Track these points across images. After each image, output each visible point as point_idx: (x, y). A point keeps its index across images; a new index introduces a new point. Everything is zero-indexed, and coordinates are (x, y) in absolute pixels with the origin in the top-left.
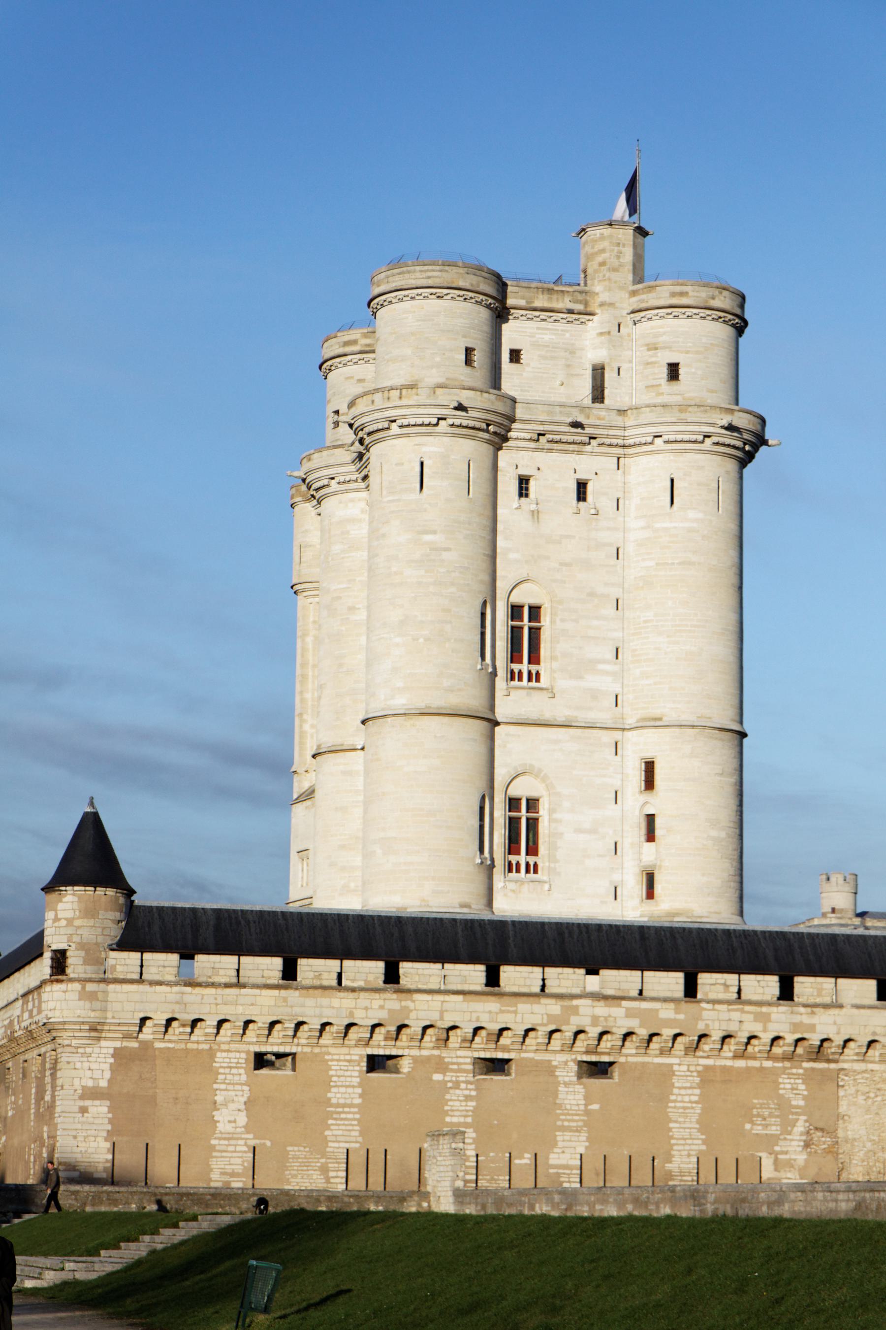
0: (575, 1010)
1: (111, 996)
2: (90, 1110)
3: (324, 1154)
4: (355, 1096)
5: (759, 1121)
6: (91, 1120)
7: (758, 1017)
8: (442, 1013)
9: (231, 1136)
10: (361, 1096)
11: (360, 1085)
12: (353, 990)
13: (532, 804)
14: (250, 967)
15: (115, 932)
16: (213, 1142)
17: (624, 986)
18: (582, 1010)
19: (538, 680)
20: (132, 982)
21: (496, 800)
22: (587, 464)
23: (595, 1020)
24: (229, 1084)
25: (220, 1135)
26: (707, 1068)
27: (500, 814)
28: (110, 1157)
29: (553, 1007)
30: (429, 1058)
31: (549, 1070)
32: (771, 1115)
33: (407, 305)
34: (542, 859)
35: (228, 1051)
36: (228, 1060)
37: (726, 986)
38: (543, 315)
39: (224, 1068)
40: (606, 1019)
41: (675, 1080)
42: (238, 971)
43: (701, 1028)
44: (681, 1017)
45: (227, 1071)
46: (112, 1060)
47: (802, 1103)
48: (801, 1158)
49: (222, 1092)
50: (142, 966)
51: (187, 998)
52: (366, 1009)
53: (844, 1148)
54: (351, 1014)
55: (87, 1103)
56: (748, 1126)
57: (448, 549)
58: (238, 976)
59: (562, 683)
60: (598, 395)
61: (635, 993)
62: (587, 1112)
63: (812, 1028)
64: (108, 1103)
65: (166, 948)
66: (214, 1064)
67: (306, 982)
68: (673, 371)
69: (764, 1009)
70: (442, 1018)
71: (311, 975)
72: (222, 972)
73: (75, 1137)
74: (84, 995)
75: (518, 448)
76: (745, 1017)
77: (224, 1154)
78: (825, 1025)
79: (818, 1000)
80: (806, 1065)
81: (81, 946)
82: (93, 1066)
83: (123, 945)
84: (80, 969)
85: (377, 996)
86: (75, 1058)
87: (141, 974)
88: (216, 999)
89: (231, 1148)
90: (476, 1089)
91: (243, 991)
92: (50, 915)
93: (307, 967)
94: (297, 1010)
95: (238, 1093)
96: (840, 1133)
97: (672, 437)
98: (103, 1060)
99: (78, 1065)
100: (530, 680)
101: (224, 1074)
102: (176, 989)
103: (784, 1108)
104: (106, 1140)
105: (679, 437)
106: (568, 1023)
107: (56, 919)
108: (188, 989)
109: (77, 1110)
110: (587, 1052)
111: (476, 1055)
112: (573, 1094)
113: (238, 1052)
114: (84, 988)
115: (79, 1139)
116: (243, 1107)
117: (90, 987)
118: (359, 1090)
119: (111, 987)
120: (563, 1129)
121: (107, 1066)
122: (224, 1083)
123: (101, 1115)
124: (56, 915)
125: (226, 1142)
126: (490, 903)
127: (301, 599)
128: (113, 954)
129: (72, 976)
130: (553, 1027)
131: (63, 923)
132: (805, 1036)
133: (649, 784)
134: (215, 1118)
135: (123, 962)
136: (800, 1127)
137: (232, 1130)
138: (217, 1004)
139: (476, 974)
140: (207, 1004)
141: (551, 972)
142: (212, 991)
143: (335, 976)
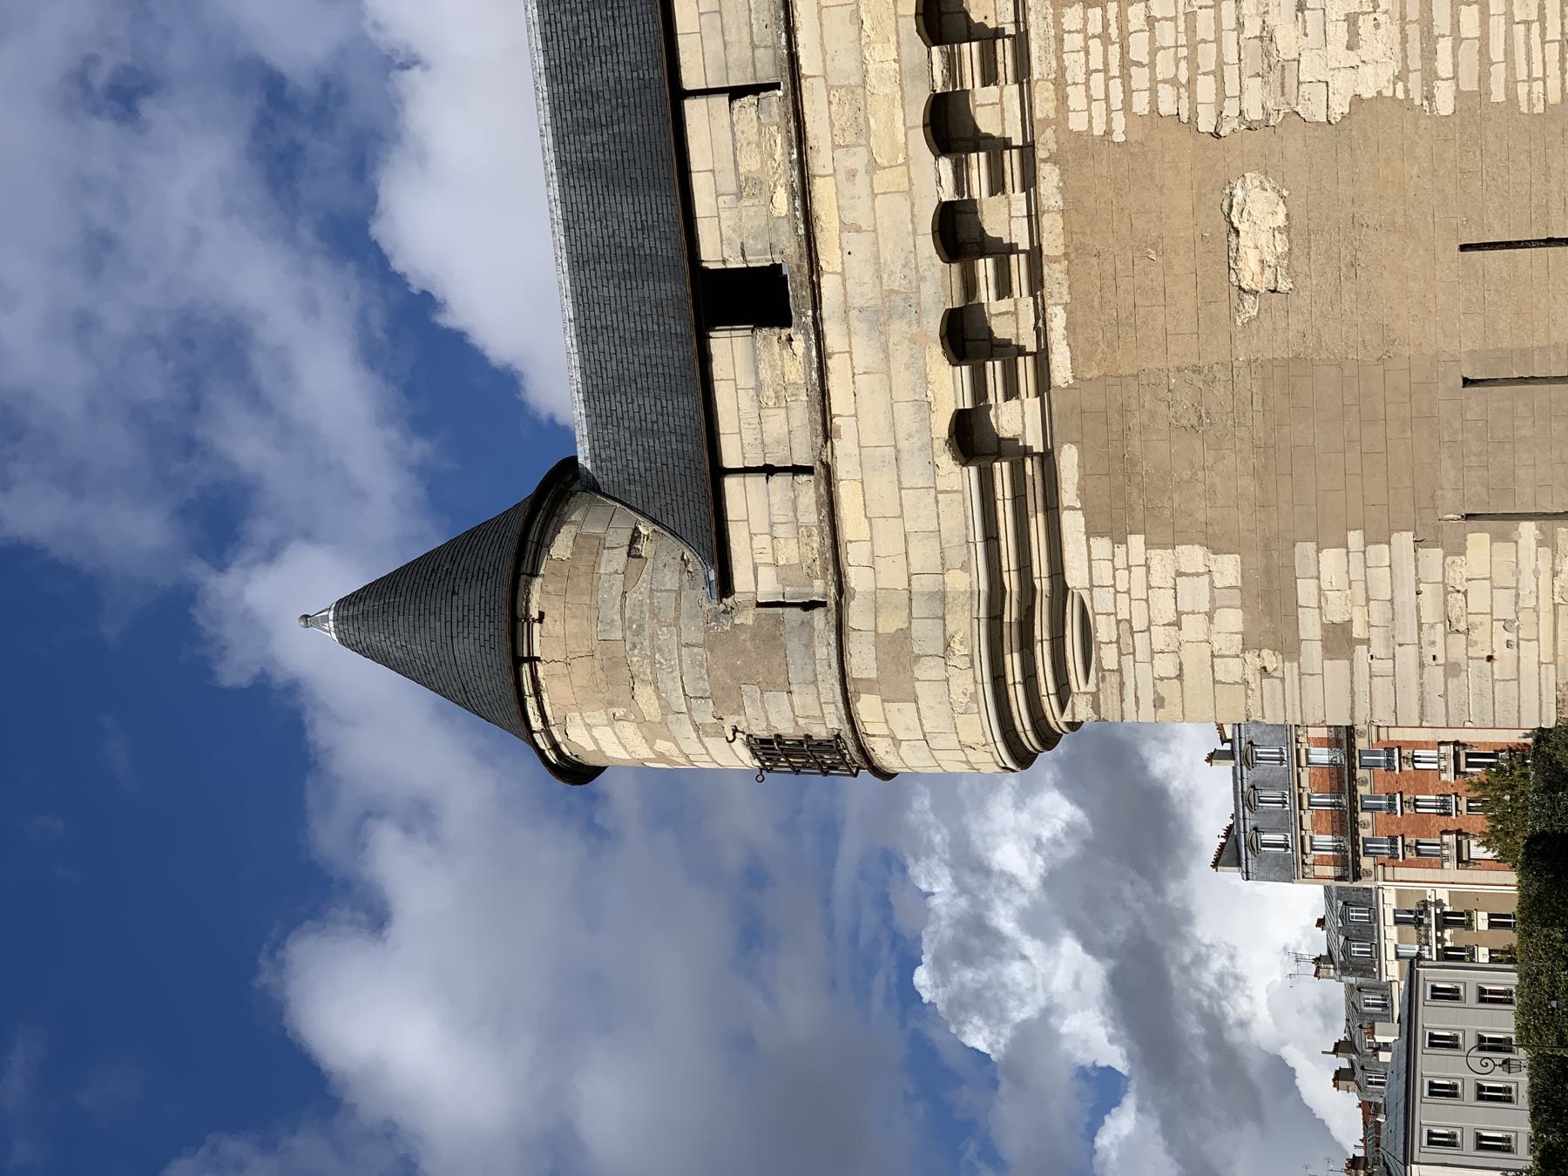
2: (1336, 615)
6: (1378, 612)
9: (1414, 32)
14: (714, 45)
15: (669, 565)
16: (1445, 104)
20: (830, 505)
24: (1194, 66)
25: (1415, 80)
28: (1528, 529)
35: (1060, 83)
36: (1098, 80)
39: (1128, 93)
42: (736, 93)
45: (1140, 78)
46: (1136, 541)
49: (1232, 88)
50: (769, 470)
51: (864, 293)
55: (1310, 626)
58: (755, 89)
64: (1305, 549)
66: (1119, 137)
72: (750, 163)
73: (1452, 669)
74: (899, 689)
77: (1497, 53)
81: (724, 696)
82: (1164, 608)
84: (803, 698)
86: (1140, 676)
87: (797, 470)
88: (852, 174)
91: (807, 65)
95: (1229, 21)
98: (1139, 573)
99: (1166, 666)
101: (1153, 91)
102: (833, 340)
104: (1460, 550)
108: (828, 285)
109: (1343, 664)
113: (1060, 40)
114: (871, 686)
119: (857, 578)
122: (1191, 82)
123: (1357, 572)
125: (1444, 46)
128: (742, 579)
134: (1340, 107)
135: (763, 541)
137: (1390, 30)
138: (873, 166)
142: (822, 190)
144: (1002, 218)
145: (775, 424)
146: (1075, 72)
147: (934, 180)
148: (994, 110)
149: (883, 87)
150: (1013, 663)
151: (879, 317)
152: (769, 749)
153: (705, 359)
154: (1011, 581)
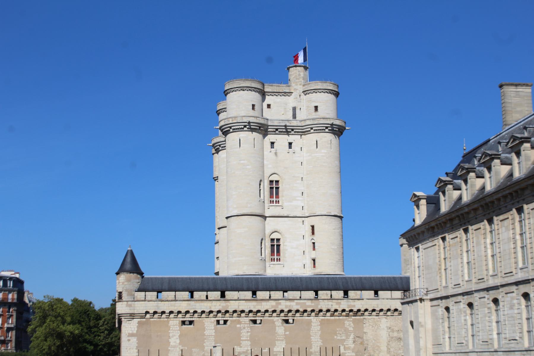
0: (280, 304)
1: (136, 306)
3: (204, 351)
4: (213, 333)
5: (339, 335)
7: (337, 304)
8: (239, 306)
11: (214, 329)
12: (211, 301)
13: (278, 240)
15: (137, 286)
17: (295, 296)
18: (282, 304)
19: (278, 203)
21: (266, 240)
22: (292, 138)
23: (286, 307)
26: (322, 320)
27: (268, 244)
29: (273, 303)
30: (235, 320)
31: (273, 322)
32: (343, 333)
33: (234, 92)
34: (282, 257)
37: (327, 294)
38: (277, 94)
40: (290, 306)
41: (312, 323)
43: (320, 307)
44: (313, 304)
47: (352, 329)
48: (352, 346)
53: (366, 342)
54: (210, 308)
55: (130, 338)
56: (335, 337)
57: (248, 165)
59: (286, 204)
60: (294, 116)
61: (299, 298)
62: (285, 335)
63: (354, 306)
65: (153, 290)
67: (196, 299)
68: (316, 108)
69: (339, 301)
70: (238, 308)
74: (127, 305)
76: (333, 304)
78: (358, 305)
79: (356, 298)
80: (353, 317)
83: (139, 290)
84: (126, 297)
90: (250, 329)
92: (117, 281)
93: (196, 294)
94: (194, 307)
96: (364, 338)
97: (316, 128)
100: (276, 203)
103: (346, 330)
105: (318, 128)
106: (278, 308)
111: (250, 318)
112: (280, 328)
116: (178, 337)
117: (129, 303)
118: (214, 331)
119: (136, 302)
120: (278, 340)
126: (265, 271)
127: (216, 182)
128: (136, 293)
130: (273, 309)
131: (121, 284)
132: (352, 308)
133: (313, 233)
136: (352, 336)
139: (249, 294)
140: (166, 307)
141: (272, 293)
142: (167, 302)
143: (205, 296)
144: (164, 316)
145: (149, 297)
147: (167, 311)
148: (172, 316)
149: (176, 308)
151: (157, 306)
152: (120, 293)
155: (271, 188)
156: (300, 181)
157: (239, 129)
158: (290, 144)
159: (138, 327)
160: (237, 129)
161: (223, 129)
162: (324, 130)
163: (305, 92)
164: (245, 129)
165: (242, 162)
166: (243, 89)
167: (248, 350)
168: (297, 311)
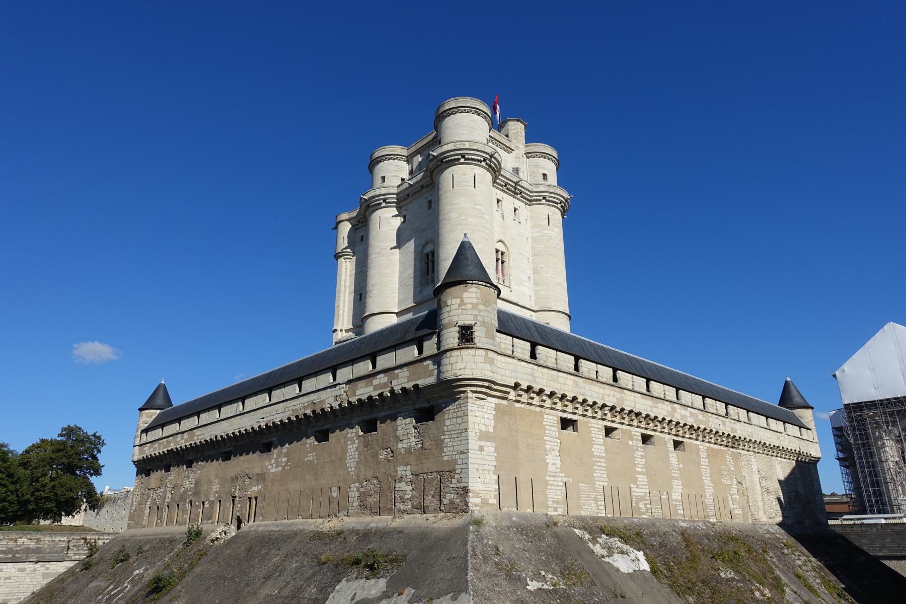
2: (485, 449)
10: (606, 451)
16: (548, 478)
35: (549, 414)
46: (494, 412)
52: (609, 395)
55: (483, 443)
59: (513, 287)
67: (585, 374)
68: (545, 175)
71: (586, 370)
72: (550, 359)
73: (477, 470)
75: (497, 188)
78: (741, 430)
81: (484, 324)
84: (484, 340)
85: (612, 388)
89: (555, 483)
99: (477, 414)
107: (462, 303)
108: (536, 367)
110: (676, 435)
112: (674, 457)
114: (487, 354)
115: (481, 471)
117: (491, 354)
119: (500, 357)
120: (674, 478)
121: (491, 417)
124: (462, 300)
129: (479, 345)
131: (470, 306)
142: (546, 370)
146: (551, 417)
150: (486, 384)
153: (527, 341)
154: (496, 387)
155: (497, 260)
156: (526, 262)
157: (475, 160)
158: (515, 210)
159: (497, 418)
160: (472, 159)
161: (445, 158)
162: (557, 203)
163: (529, 155)
164: (483, 164)
165: (478, 207)
166: (478, 112)
167: (645, 493)
168: (692, 427)
